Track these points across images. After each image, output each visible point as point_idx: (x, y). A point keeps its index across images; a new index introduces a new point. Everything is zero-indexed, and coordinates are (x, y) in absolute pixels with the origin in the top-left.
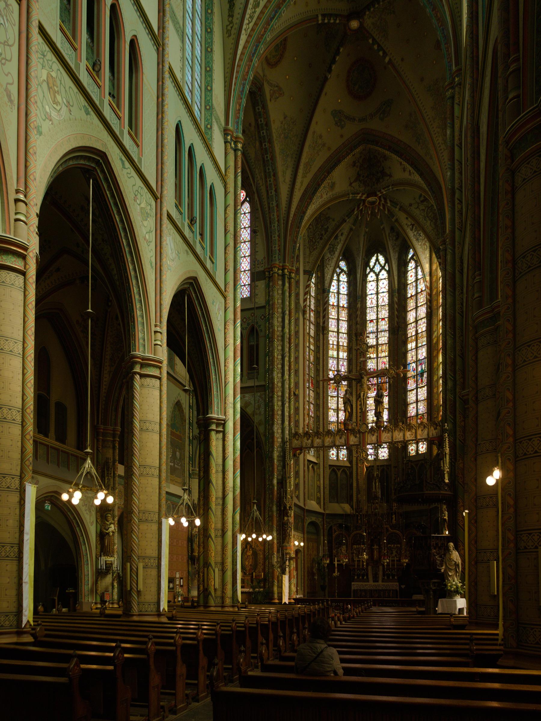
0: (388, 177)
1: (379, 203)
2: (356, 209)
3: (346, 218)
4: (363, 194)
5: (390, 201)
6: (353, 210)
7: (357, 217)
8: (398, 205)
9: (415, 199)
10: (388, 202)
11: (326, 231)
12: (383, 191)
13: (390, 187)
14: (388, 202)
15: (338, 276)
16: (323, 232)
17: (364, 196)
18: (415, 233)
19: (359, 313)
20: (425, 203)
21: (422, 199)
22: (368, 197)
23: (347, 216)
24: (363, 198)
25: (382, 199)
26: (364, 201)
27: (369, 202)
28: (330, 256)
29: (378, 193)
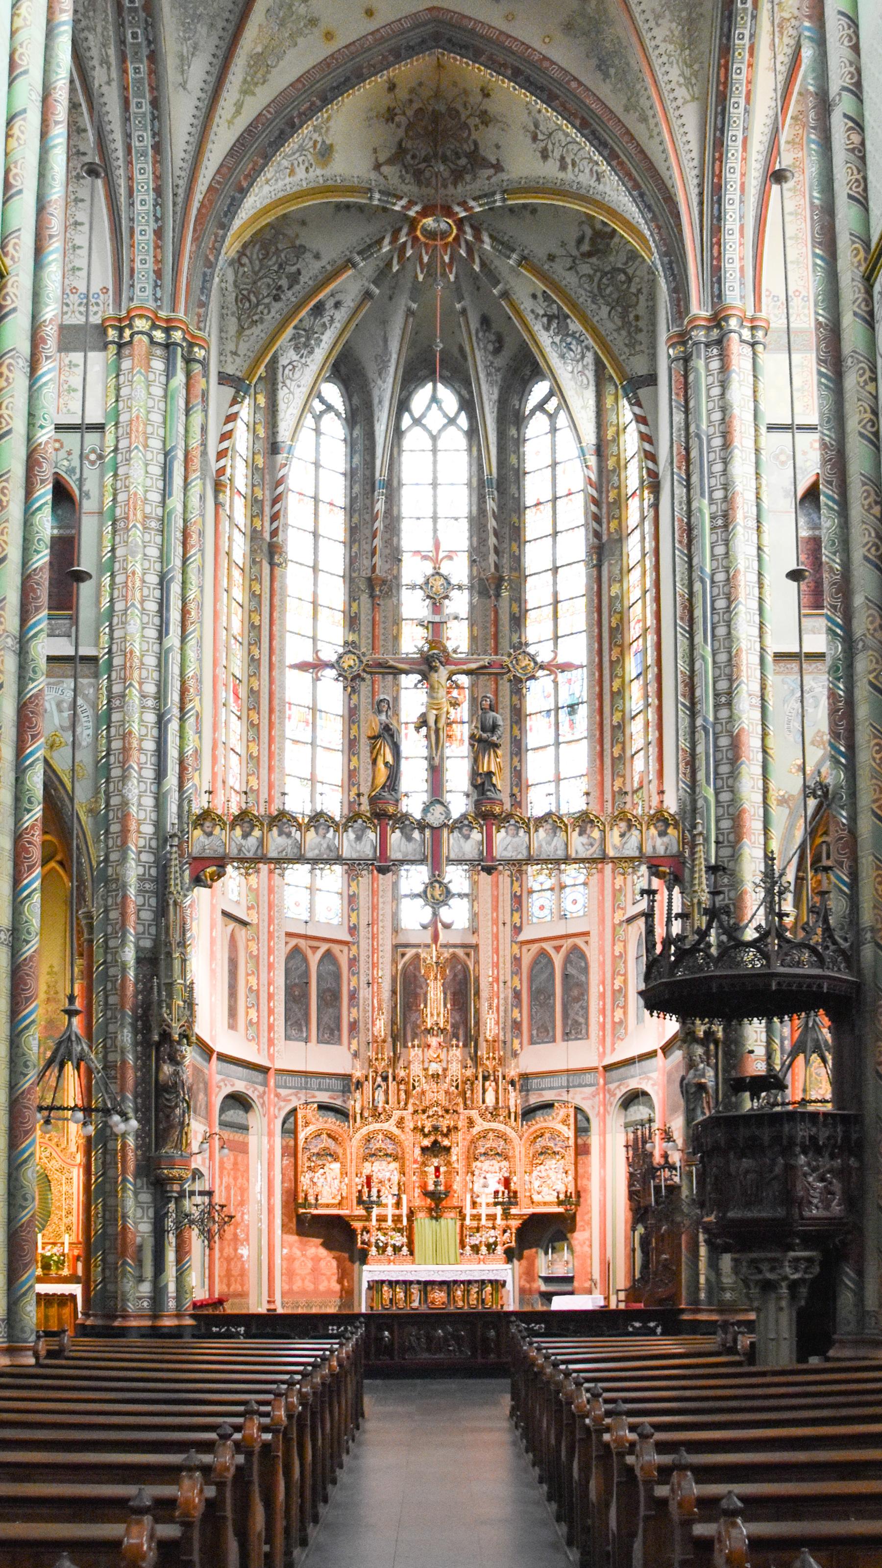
0: (492, 171)
1: (457, 239)
2: (387, 241)
3: (357, 258)
4: (411, 203)
5: (491, 237)
6: (379, 242)
7: (389, 265)
8: (513, 250)
9: (563, 244)
10: (486, 239)
11: (294, 278)
12: (472, 203)
13: (498, 197)
14: (486, 239)
15: (318, 418)
16: (284, 282)
17: (418, 208)
18: (557, 339)
19: (379, 524)
20: (594, 260)
21: (586, 247)
22: (424, 213)
23: (359, 253)
24: (412, 213)
25: (468, 229)
26: (413, 224)
27: (424, 230)
28: (295, 357)
29: (457, 209)
